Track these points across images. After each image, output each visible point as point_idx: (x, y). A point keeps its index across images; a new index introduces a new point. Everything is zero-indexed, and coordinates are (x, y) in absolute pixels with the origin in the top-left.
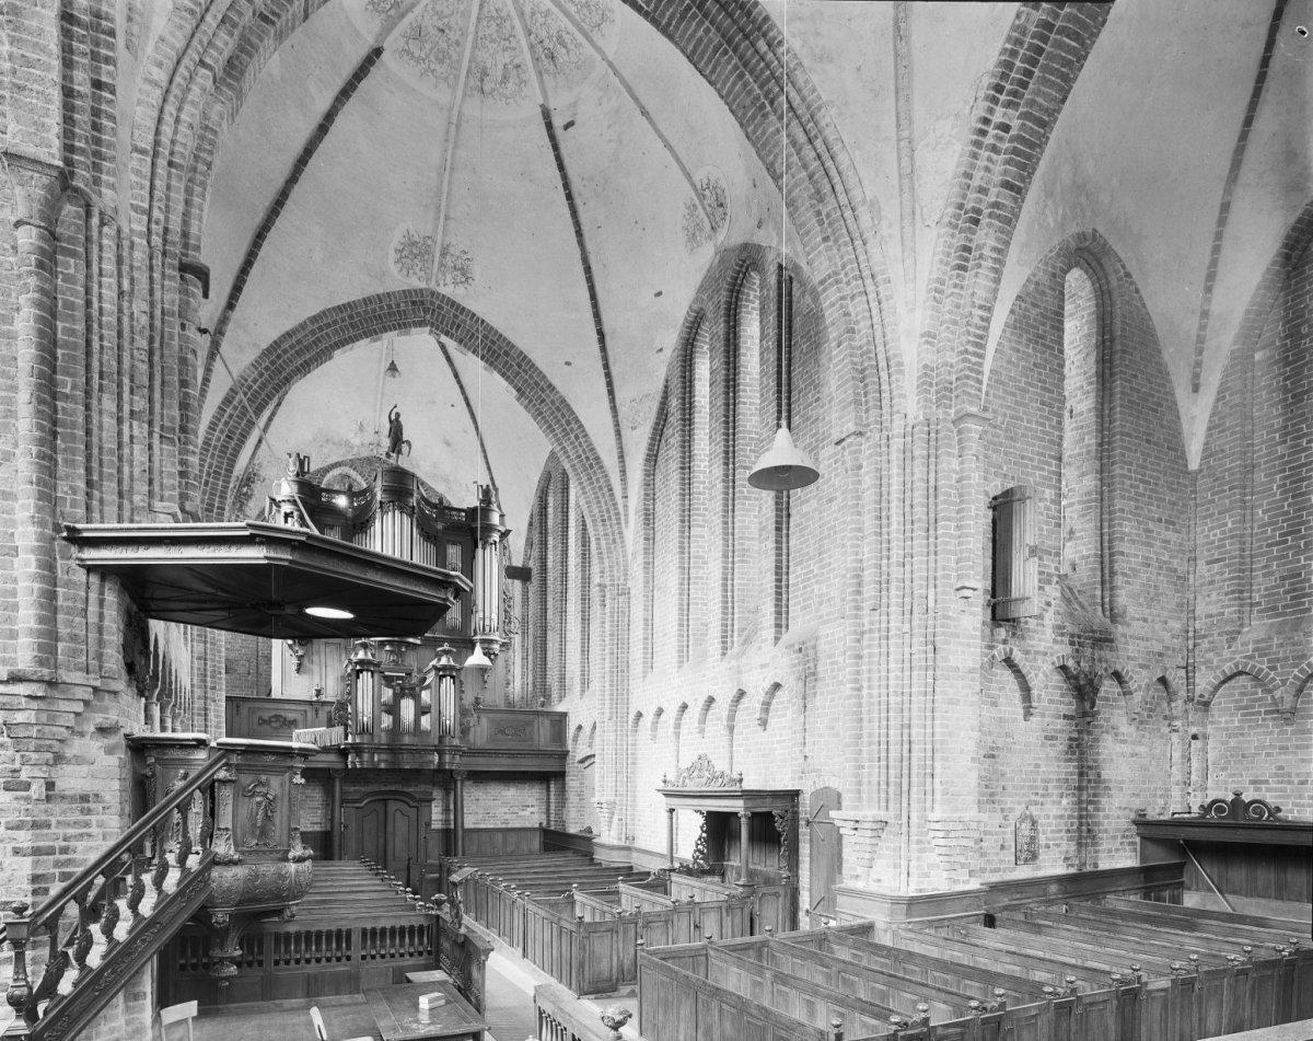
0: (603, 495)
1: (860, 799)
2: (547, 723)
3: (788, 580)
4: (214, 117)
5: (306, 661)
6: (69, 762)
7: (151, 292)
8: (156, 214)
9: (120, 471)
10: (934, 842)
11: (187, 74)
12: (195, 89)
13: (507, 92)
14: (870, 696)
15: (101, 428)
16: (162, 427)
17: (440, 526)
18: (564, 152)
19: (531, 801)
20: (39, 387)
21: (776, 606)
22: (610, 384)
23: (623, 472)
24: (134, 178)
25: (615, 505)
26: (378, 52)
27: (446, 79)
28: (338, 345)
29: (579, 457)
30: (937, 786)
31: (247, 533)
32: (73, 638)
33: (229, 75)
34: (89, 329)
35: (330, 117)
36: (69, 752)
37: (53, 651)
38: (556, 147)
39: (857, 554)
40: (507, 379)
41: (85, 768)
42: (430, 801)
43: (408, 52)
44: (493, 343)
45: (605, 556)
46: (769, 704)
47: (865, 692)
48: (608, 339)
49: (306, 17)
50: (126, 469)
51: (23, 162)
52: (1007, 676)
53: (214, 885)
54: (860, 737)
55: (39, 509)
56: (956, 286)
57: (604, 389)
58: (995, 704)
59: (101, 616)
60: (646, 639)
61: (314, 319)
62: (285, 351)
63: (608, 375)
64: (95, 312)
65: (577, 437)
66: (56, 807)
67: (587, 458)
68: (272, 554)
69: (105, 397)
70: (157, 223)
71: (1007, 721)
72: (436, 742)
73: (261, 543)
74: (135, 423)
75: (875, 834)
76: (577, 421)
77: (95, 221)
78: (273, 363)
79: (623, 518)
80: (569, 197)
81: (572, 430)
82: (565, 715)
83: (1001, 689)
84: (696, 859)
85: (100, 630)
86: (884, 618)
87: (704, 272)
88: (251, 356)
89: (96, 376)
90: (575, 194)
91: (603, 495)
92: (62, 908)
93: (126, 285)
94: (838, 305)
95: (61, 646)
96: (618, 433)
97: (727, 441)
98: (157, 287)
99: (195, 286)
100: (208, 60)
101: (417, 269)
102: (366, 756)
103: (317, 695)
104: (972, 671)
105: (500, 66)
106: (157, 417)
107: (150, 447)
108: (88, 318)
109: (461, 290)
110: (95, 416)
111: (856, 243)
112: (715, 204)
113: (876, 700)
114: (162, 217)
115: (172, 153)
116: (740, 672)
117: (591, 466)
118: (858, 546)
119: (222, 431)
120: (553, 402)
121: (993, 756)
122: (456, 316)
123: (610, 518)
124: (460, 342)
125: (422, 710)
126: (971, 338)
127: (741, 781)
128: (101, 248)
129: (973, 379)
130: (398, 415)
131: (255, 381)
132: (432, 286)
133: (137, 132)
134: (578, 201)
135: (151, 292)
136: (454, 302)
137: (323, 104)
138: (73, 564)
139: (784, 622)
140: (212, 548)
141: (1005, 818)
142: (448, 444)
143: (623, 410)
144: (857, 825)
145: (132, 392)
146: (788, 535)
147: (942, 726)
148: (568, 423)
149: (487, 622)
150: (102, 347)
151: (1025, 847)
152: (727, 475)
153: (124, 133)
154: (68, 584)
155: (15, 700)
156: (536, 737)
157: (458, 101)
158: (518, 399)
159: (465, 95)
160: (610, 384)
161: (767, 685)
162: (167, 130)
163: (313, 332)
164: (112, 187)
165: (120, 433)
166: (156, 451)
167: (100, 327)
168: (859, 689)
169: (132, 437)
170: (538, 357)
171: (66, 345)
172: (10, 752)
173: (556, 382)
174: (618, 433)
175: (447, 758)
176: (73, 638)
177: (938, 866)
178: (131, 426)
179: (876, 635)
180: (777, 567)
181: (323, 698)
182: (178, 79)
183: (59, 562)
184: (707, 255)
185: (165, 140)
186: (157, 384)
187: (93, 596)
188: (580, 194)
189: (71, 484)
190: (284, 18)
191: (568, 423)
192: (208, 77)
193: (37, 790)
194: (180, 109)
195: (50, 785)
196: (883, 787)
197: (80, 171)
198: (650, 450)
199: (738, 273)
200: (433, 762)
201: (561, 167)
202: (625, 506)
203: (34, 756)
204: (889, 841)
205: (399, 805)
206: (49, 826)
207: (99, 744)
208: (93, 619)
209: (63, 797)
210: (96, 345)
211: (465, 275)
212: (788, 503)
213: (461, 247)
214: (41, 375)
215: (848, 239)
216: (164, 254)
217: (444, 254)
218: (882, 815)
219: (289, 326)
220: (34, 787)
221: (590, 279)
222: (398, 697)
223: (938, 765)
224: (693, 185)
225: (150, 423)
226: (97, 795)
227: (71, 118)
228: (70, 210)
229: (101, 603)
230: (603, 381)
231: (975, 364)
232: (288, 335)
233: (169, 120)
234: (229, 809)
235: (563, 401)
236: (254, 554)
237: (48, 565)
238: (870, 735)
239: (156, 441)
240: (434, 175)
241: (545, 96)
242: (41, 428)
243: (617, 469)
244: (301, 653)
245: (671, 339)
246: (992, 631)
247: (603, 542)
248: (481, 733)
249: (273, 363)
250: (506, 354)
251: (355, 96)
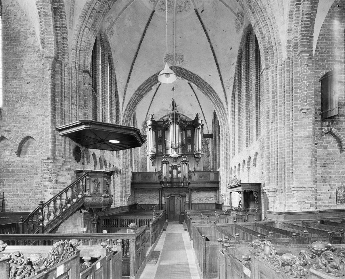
0: (221, 109)
1: (270, 182)
2: (213, 174)
3: (260, 121)
4: (90, 38)
5: (154, 164)
6: (60, 176)
7: (76, 78)
8: (77, 62)
9: (69, 116)
10: (294, 195)
11: (83, 30)
12: (85, 33)
13: (186, 9)
14: (272, 150)
15: (65, 107)
16: (79, 106)
17: (185, 126)
18: (202, 19)
19: (212, 196)
20: (52, 101)
21: (256, 129)
22: (221, 78)
23: (227, 101)
24: (72, 55)
25: (225, 111)
26: (154, 12)
27: (171, 12)
28: (153, 86)
29: (215, 100)
30: (294, 176)
31: (80, 123)
32: (59, 150)
33: (93, 27)
34: (62, 88)
35: (145, 32)
36: (60, 174)
37: (55, 153)
38: (200, 19)
39: (267, 106)
40: (194, 84)
41: (64, 177)
42: (186, 196)
43: (161, 9)
44: (190, 75)
45: (223, 126)
46: (256, 159)
47: (270, 148)
48: (220, 66)
49: (110, 8)
50: (71, 115)
51: (48, 58)
52: (332, 139)
53: (85, 201)
54: (269, 163)
55: (52, 125)
56: (296, 11)
57: (219, 79)
58: (326, 149)
59: (65, 146)
60: (233, 147)
61: (147, 80)
62: (141, 90)
63: (220, 75)
64: (63, 84)
65: (213, 95)
66: (58, 185)
67: (217, 100)
68: (86, 127)
69: (66, 101)
70: (77, 63)
71: (332, 154)
72: (182, 180)
73: (84, 125)
74: (73, 106)
75: (274, 193)
76: (213, 90)
77: (63, 66)
78: (138, 93)
80: (205, 30)
81: (212, 93)
82: (218, 172)
83: (328, 143)
84: (239, 207)
85: (65, 149)
86: (276, 124)
87: (241, 38)
88: (133, 92)
89: (63, 97)
90: (207, 29)
91: (221, 109)
92: (50, 202)
93: (70, 78)
94: (259, 31)
95: (57, 152)
96: (224, 91)
97: (247, 84)
98: (77, 77)
99: (87, 75)
100: (87, 26)
101: (170, 62)
102: (165, 184)
103: (155, 171)
104: (308, 137)
105: (184, 3)
106: (78, 104)
107: (76, 110)
108: (62, 86)
109: (181, 64)
110: (63, 105)
111: (262, 10)
112: (241, 17)
113: (274, 151)
114: (78, 62)
115: (80, 48)
116: (249, 151)
117: (218, 101)
118: (268, 103)
119: (128, 111)
120: (206, 87)
121: (325, 166)
122: (180, 71)
123: (224, 115)
124: (182, 77)
125: (179, 172)
126: (303, 26)
127: (241, 181)
128: (65, 71)
129: (305, 39)
130: (174, 100)
131: (135, 98)
132: (174, 65)
133: (72, 46)
134: (207, 31)
135: (76, 78)
136: (179, 67)
137: (143, 29)
138: (59, 135)
139: (259, 134)
140: (79, 127)
141: (331, 188)
142: (191, 105)
143: (225, 84)
144: (269, 191)
145: (72, 99)
146: (260, 107)
147: (295, 156)
148: (211, 91)
149: (198, 149)
150: (65, 91)
151: (341, 198)
152: (247, 94)
153: (70, 47)
154: (58, 140)
155: (49, 163)
156: (210, 178)
157: (175, 16)
158: (198, 88)
159: (176, 14)
160: (221, 78)
161: (254, 153)
162: (79, 43)
163: (147, 84)
164: (67, 58)
165: (69, 108)
166: (78, 111)
167: (65, 87)
168: (269, 148)
169: (72, 109)
170: (202, 76)
171: (57, 92)
172: (49, 174)
173: (207, 81)
174: (224, 91)
175: (185, 184)
176: (59, 150)
177: (296, 203)
178: (72, 106)
179: (273, 130)
180: (256, 117)
181: (157, 171)
182: (81, 32)
183: (56, 135)
184: (241, 32)
185: (78, 46)
186: (78, 97)
187: (63, 142)
188: (208, 29)
189: (58, 119)
190: (103, 11)
191: (211, 91)
192: (87, 30)
193: (54, 181)
194: (82, 38)
195: (57, 180)
196: (276, 178)
197: (60, 57)
198: (232, 93)
199: (248, 34)
200: (181, 185)
201: (202, 23)
202: (228, 111)
203: (53, 174)
204: (279, 195)
205: (179, 198)
206: (56, 189)
207: (66, 172)
208: (63, 146)
209: (59, 183)
210: (63, 91)
211: (182, 60)
212: (260, 97)
213: (180, 53)
214: (52, 99)
215: (260, 10)
216: (79, 70)
217: (176, 56)
218: (276, 187)
219: (141, 84)
220: (53, 181)
221: (213, 51)
222: (172, 169)
223: (294, 169)
224: (235, 14)
225: (76, 106)
226: (66, 183)
227: (58, 47)
228: (58, 65)
229: (65, 143)
230: (219, 77)
231: (306, 34)
232: (141, 86)
233: (79, 41)
234: (89, 185)
235: (209, 86)
236: (83, 127)
237: (54, 136)
238: (272, 162)
239: (78, 109)
240: (171, 37)
241: (195, 6)
242: (52, 109)
243: (225, 101)
244: (153, 161)
245: (235, 60)
246: (322, 124)
247: (222, 122)
248: (195, 178)
249: (138, 93)
250: (194, 77)
251: (150, 24)
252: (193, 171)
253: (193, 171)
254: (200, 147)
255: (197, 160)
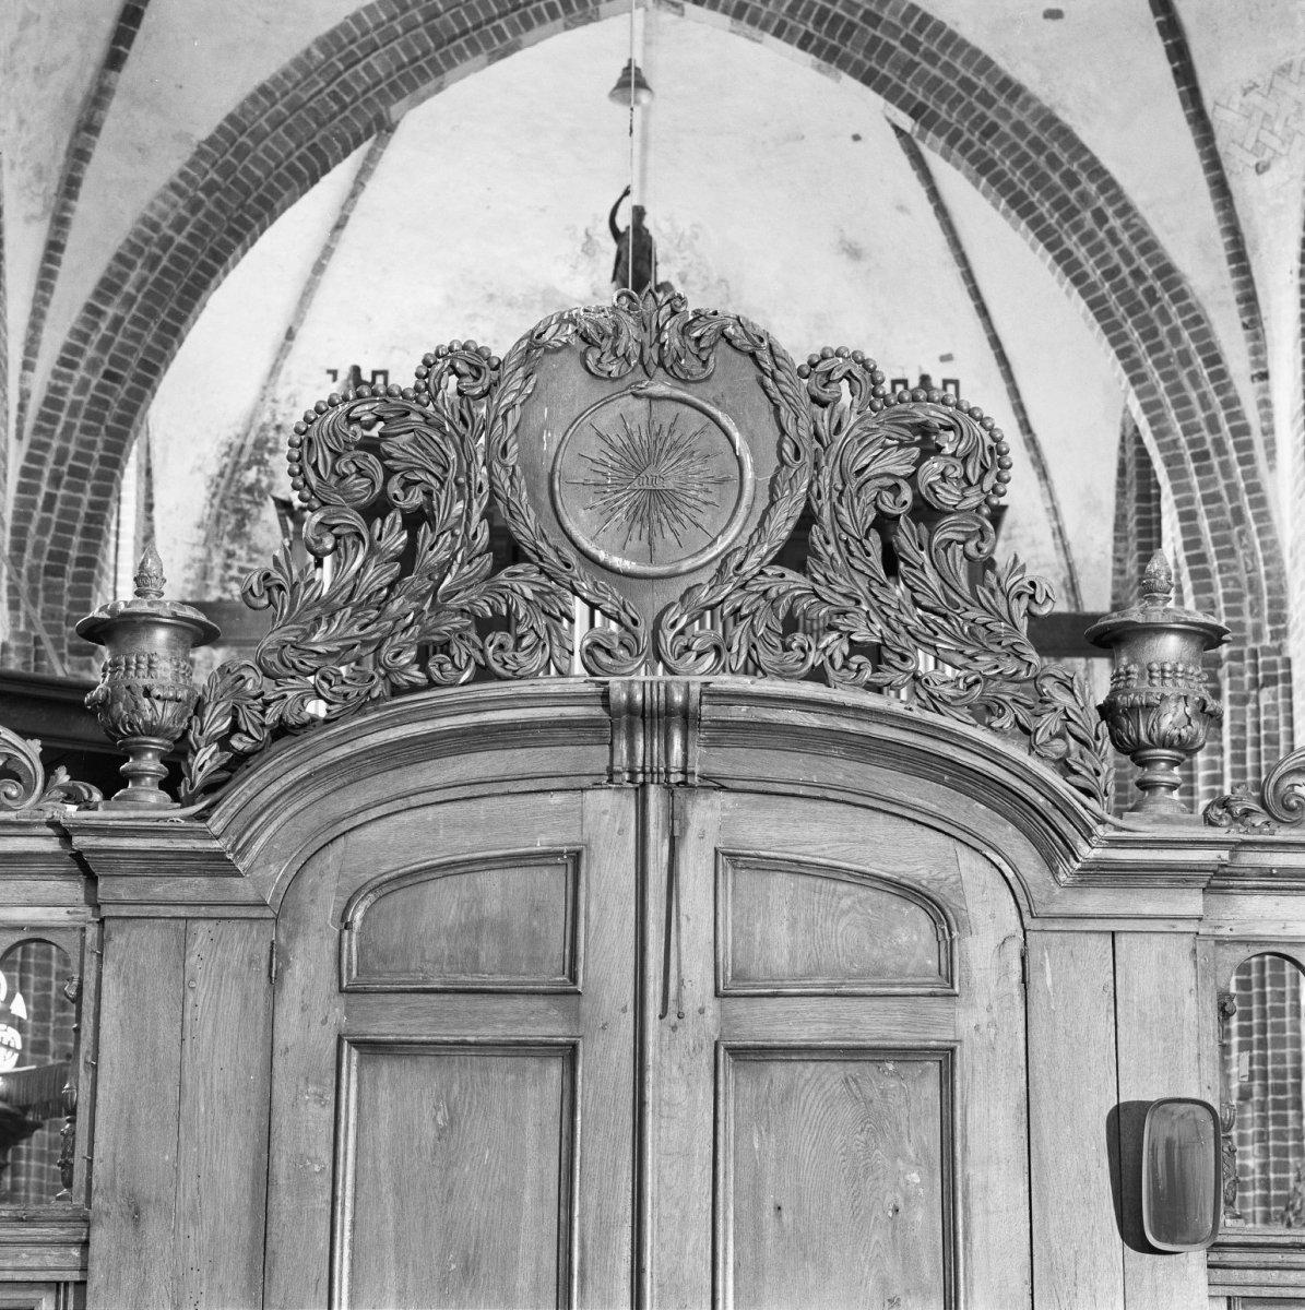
25: (1231, 403)
57: (1163, 69)
65: (1100, 218)
76: (1096, 171)
79: (1258, 440)
81: (1084, 197)
96: (1221, 189)
123: (1220, 446)
130: (639, 213)
142: (854, 253)
143: (1225, 119)
174: (1221, 189)
202: (1265, 404)
230: (1157, 46)
235: (1049, 121)
243: (1232, 295)
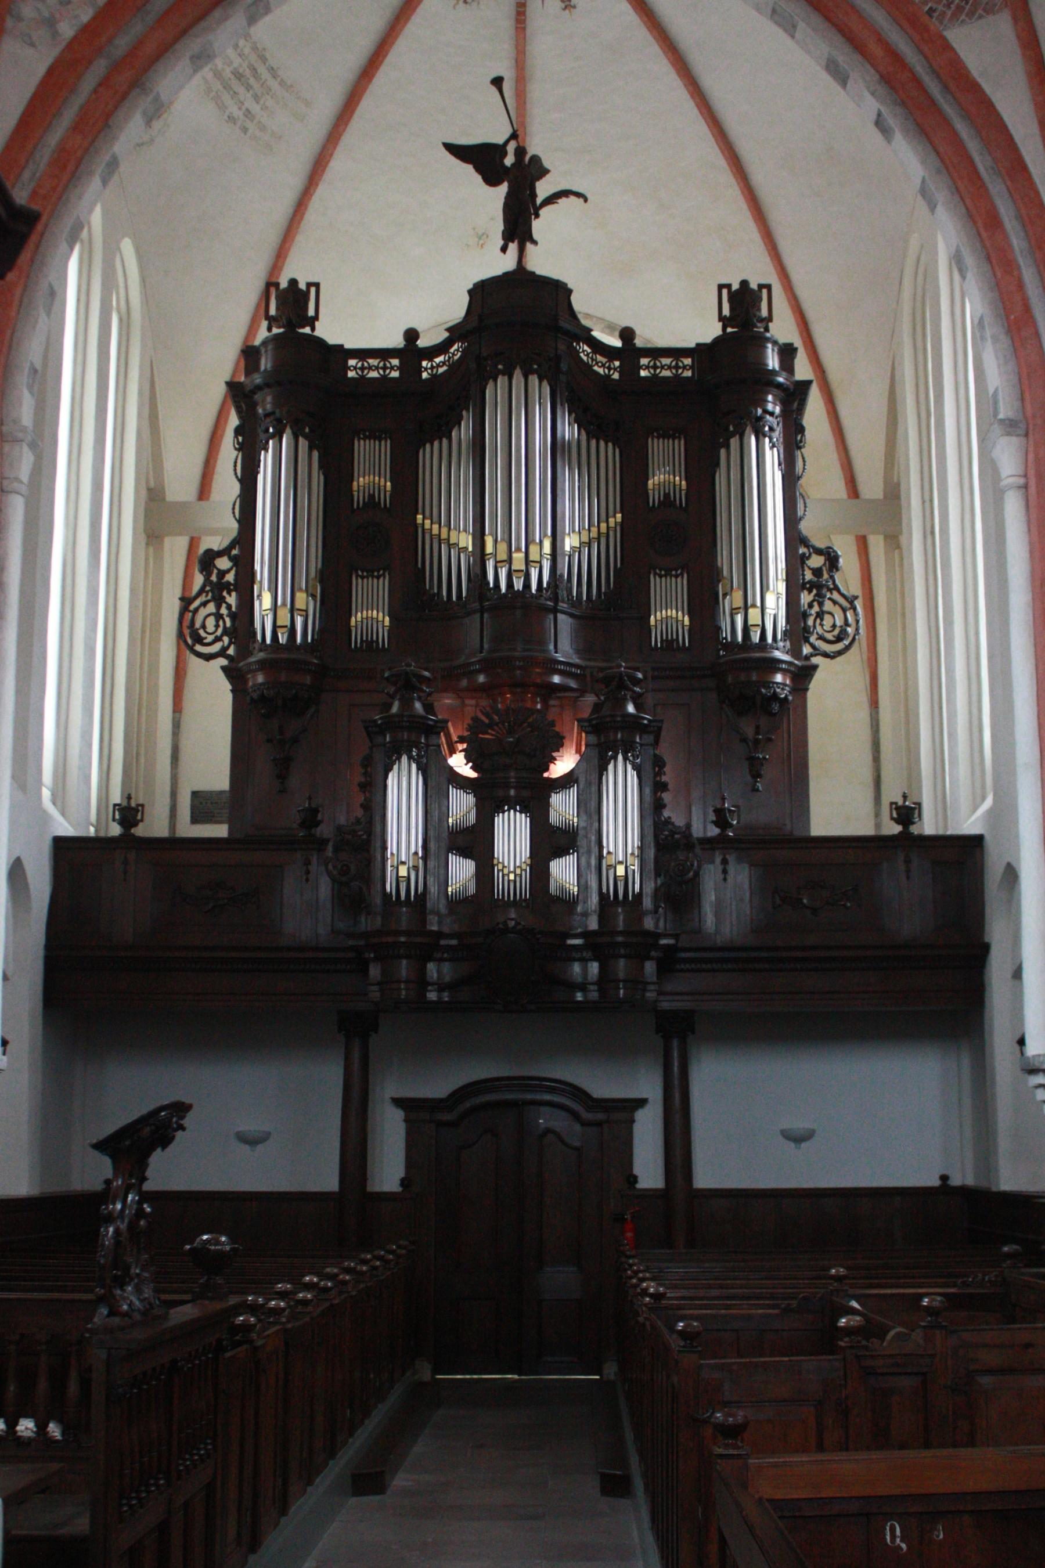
72: (593, 924)
252: (714, 831)
253: (714, 831)
254: (775, 603)
255: (750, 732)
